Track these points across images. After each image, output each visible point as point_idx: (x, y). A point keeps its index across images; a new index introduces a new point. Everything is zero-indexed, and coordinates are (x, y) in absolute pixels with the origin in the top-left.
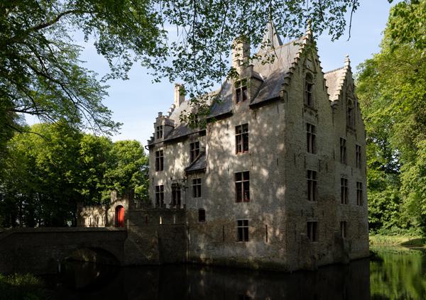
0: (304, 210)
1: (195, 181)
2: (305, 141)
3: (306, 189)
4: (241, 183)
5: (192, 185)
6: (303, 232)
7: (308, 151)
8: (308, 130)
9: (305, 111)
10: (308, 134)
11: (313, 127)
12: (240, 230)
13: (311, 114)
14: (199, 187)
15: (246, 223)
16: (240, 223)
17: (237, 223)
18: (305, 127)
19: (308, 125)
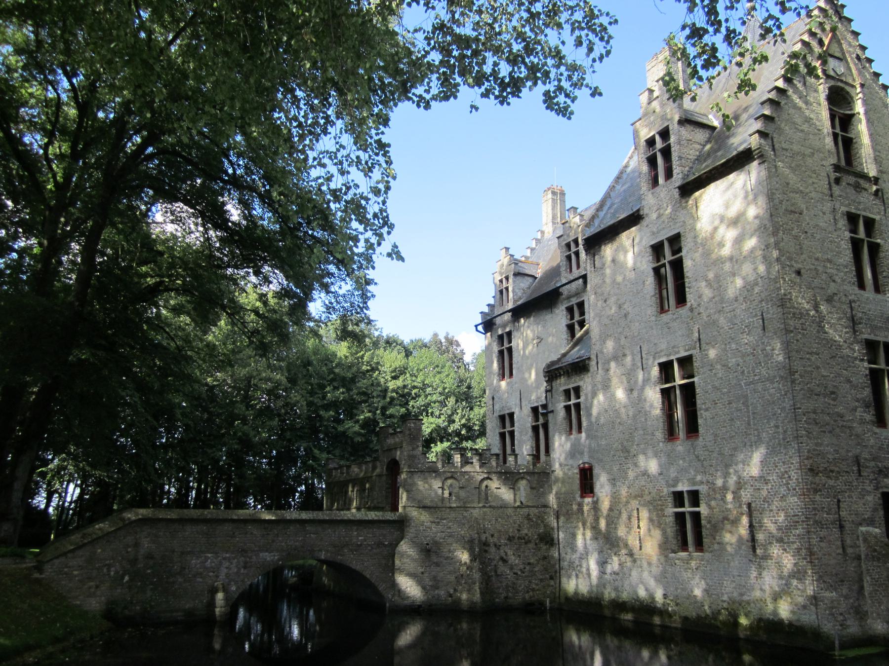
0: (865, 455)
1: (567, 393)
2: (847, 256)
3: (867, 392)
4: (674, 387)
5: (563, 404)
6: (871, 522)
7: (862, 285)
8: (854, 231)
9: (837, 181)
10: (856, 245)
11: (870, 224)
12: (680, 518)
13: (858, 188)
14: (578, 406)
15: (695, 497)
16: (678, 498)
17: (670, 500)
18: (843, 223)
19: (852, 219)
